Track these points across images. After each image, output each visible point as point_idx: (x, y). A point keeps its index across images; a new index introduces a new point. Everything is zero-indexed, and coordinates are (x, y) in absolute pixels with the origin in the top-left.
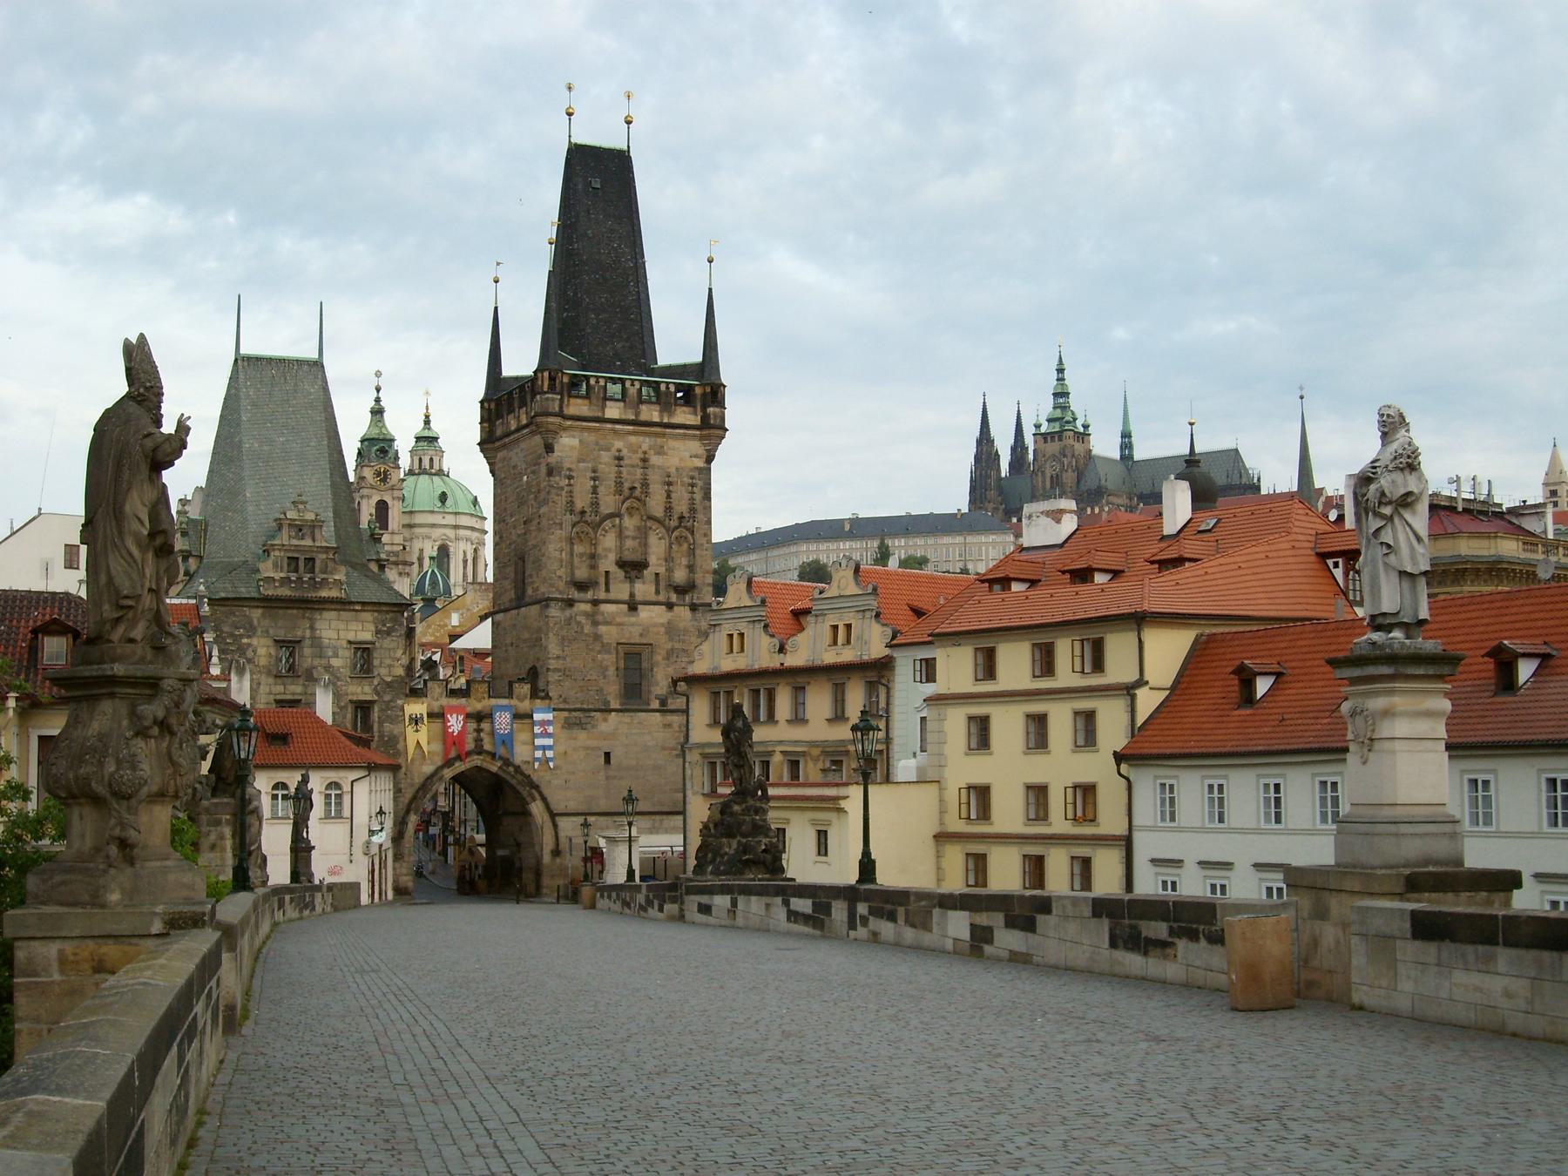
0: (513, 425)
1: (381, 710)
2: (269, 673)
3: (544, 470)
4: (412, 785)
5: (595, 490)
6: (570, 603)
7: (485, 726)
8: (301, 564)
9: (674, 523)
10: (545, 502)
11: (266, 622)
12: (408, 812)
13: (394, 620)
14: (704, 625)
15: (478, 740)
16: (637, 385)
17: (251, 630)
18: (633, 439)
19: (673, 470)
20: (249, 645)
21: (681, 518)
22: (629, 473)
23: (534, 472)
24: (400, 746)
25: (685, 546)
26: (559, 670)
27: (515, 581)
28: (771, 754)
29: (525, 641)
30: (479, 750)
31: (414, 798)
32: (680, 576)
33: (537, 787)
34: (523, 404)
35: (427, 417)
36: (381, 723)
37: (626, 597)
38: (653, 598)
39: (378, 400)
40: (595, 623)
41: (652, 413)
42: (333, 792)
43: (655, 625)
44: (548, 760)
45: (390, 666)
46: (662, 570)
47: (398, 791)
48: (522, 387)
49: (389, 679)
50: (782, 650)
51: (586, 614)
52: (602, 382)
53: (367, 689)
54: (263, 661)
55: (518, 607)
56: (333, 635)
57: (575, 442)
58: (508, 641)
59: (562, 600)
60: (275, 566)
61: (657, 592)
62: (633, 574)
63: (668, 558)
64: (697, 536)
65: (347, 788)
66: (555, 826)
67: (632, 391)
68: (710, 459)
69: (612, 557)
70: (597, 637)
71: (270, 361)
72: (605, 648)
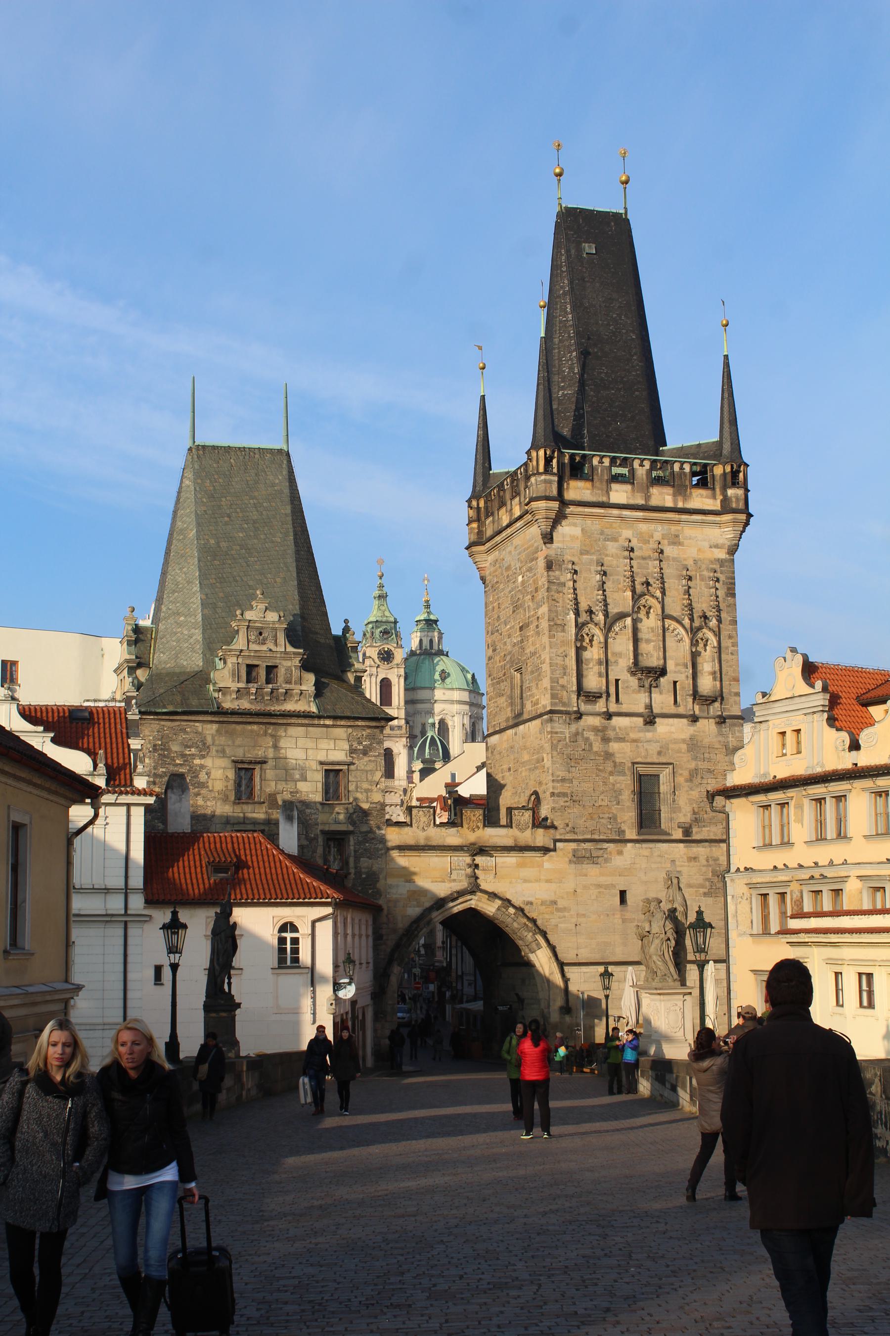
0: (505, 521)
2: (225, 799)
3: (541, 563)
8: (262, 673)
11: (222, 740)
12: (390, 962)
13: (371, 737)
14: (732, 741)
16: (647, 464)
17: (204, 749)
18: (643, 527)
19: (690, 563)
20: (202, 767)
23: (530, 570)
24: (381, 885)
26: (564, 795)
27: (511, 697)
28: (844, 879)
30: (474, 888)
31: (398, 946)
34: (516, 493)
35: (427, 601)
37: (641, 709)
38: (673, 710)
39: (381, 586)
40: (606, 740)
41: (663, 496)
42: (288, 936)
43: (676, 741)
45: (367, 791)
47: (378, 938)
48: (513, 475)
50: (855, 746)
51: (596, 730)
52: (607, 462)
54: (219, 786)
55: (516, 725)
57: (577, 531)
58: (505, 767)
59: (567, 713)
65: (304, 929)
67: (641, 471)
68: (733, 550)
70: (608, 756)
71: (228, 449)
72: (618, 769)
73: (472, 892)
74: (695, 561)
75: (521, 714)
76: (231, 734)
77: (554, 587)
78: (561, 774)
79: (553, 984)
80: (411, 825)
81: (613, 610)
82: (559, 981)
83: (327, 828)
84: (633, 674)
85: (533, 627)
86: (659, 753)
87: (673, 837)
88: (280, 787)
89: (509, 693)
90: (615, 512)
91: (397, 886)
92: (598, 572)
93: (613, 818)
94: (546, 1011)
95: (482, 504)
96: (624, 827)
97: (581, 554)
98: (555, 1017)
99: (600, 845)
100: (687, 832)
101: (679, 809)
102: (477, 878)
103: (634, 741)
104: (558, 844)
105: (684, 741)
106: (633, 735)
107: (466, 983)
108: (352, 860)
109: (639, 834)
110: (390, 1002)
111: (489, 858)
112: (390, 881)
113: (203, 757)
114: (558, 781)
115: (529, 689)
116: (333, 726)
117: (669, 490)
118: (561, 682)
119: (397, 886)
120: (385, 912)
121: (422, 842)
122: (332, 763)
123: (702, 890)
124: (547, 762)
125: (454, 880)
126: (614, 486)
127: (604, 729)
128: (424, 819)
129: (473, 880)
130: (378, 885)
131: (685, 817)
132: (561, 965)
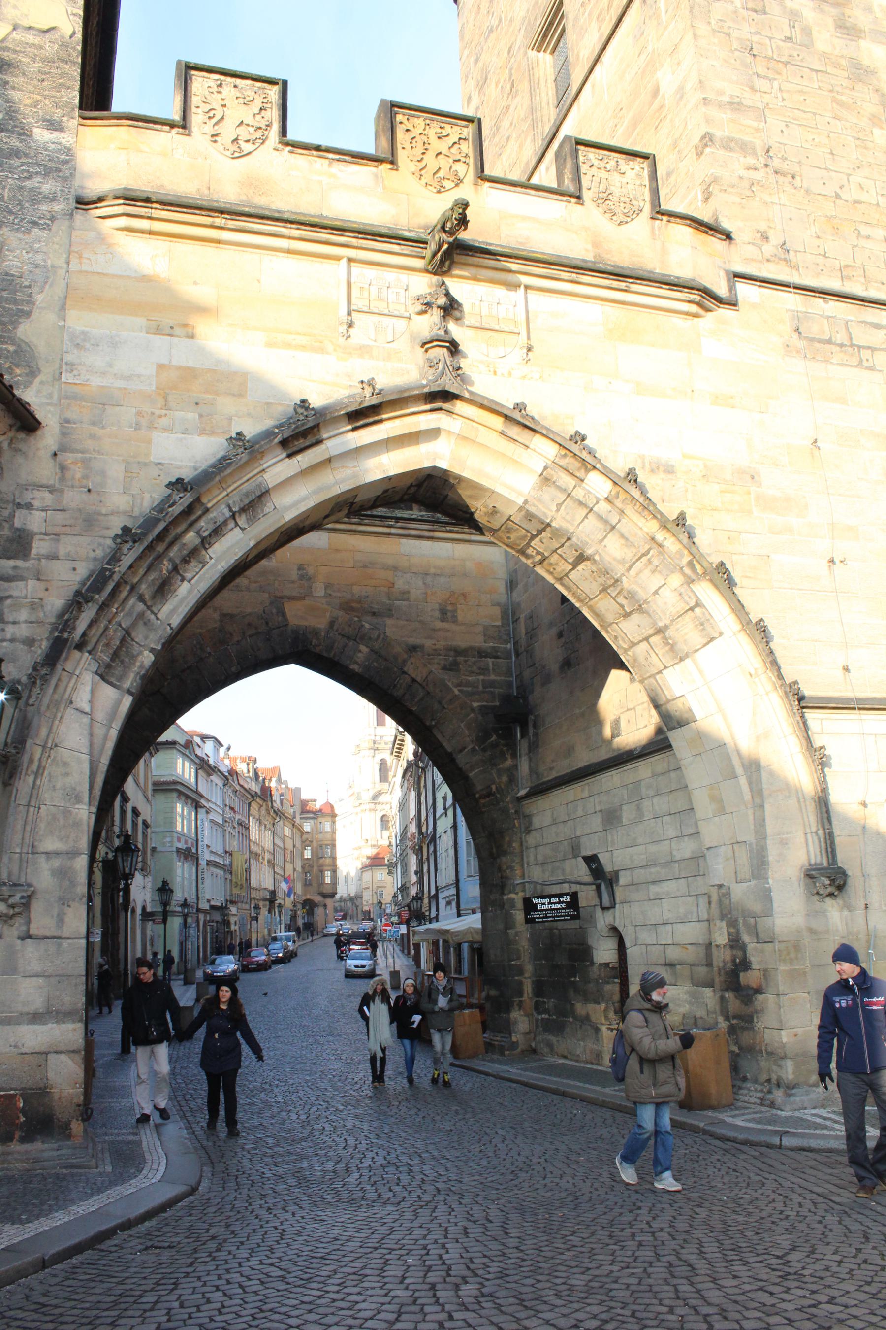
26: (745, 148)
73: (440, 397)
79: (772, 774)
80: (183, 124)
82: (798, 772)
91: (114, 344)
94: (739, 892)
98: (789, 908)
102: (454, 348)
104: (743, 289)
107: (442, 903)
110: (50, 844)
111: (500, 292)
112: (78, 320)
114: (721, 106)
119: (114, 344)
120: (49, 437)
121: (229, 193)
125: (363, 350)
129: (441, 353)
130: (24, 330)
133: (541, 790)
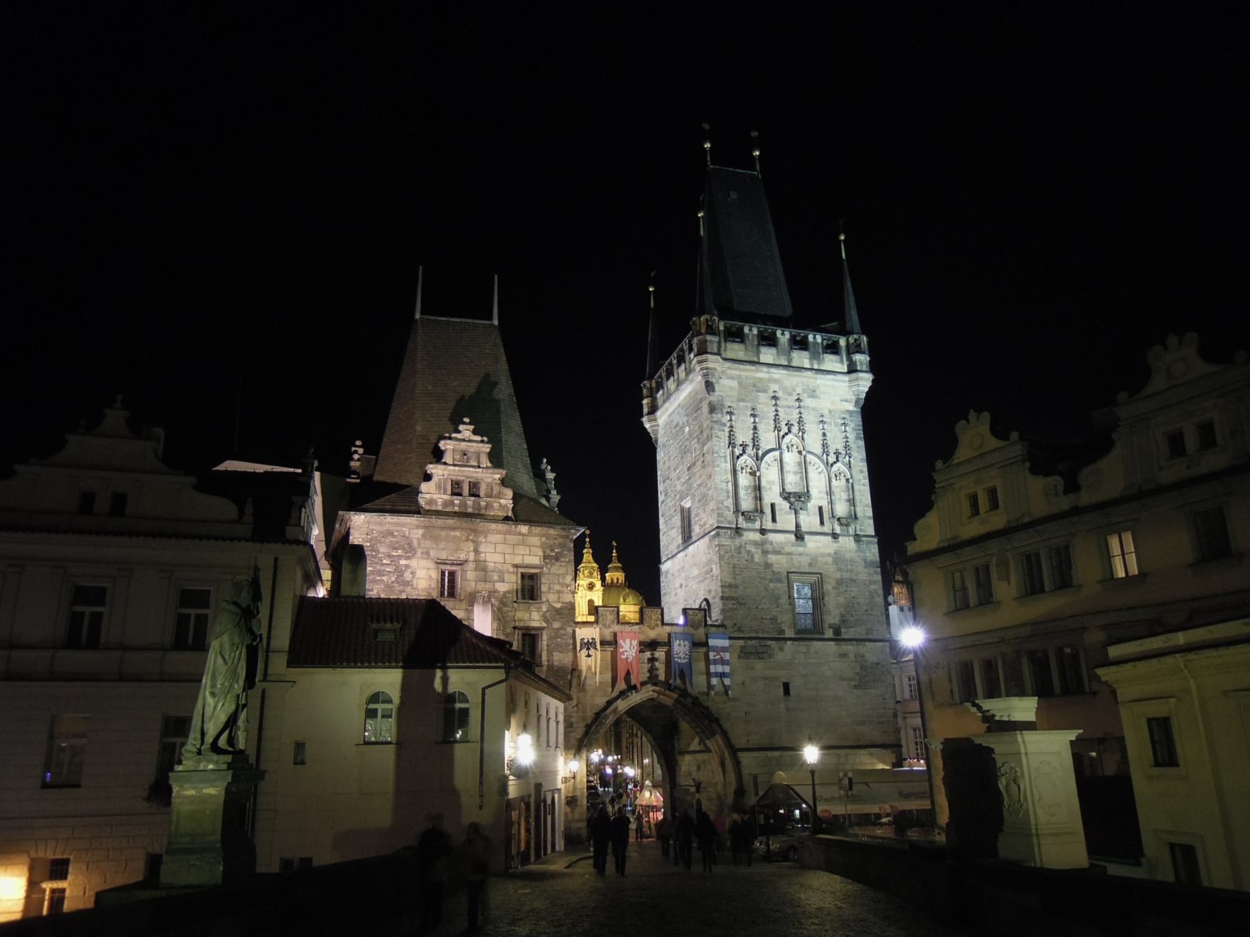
1: (550, 638)
3: (705, 409)
4: (584, 719)
5: (755, 428)
6: (738, 531)
7: (660, 654)
9: (832, 459)
10: (709, 438)
11: (428, 543)
15: (652, 670)
17: (410, 551)
19: (826, 412)
20: (407, 566)
21: (837, 454)
22: (786, 413)
23: (695, 419)
25: (844, 480)
27: (683, 527)
29: (693, 578)
32: (841, 509)
33: (717, 721)
36: (550, 653)
38: (819, 529)
40: (765, 552)
43: (823, 555)
44: (726, 689)
45: (559, 592)
46: (825, 504)
49: (558, 606)
50: (1072, 487)
51: (756, 543)
52: (755, 331)
53: (535, 615)
56: (499, 558)
57: (734, 384)
58: (677, 585)
60: (439, 487)
61: (822, 523)
62: (798, 505)
63: (830, 493)
64: (854, 473)
66: (737, 763)
69: (777, 489)
70: (768, 566)
72: (776, 578)
74: (830, 412)
75: (690, 537)
76: (436, 539)
77: (716, 426)
78: (729, 580)
81: (765, 446)
83: (522, 624)
84: (785, 499)
85: (699, 463)
86: (810, 565)
87: (826, 636)
88: (481, 586)
89: (679, 524)
90: (765, 369)
92: (754, 416)
93: (774, 619)
95: (654, 385)
96: (783, 627)
97: (740, 400)
99: (764, 643)
100: (837, 632)
101: (829, 613)
103: (790, 554)
105: (829, 555)
106: (787, 549)
108: (544, 655)
109: (798, 632)
113: (408, 558)
115: (697, 515)
116: (530, 534)
117: (805, 354)
118: (726, 503)
122: (527, 567)
123: (853, 683)
124: (716, 571)
126: (763, 349)
127: (763, 543)
128: (611, 618)
131: (832, 618)
132: (734, 751)
133: (683, 753)
